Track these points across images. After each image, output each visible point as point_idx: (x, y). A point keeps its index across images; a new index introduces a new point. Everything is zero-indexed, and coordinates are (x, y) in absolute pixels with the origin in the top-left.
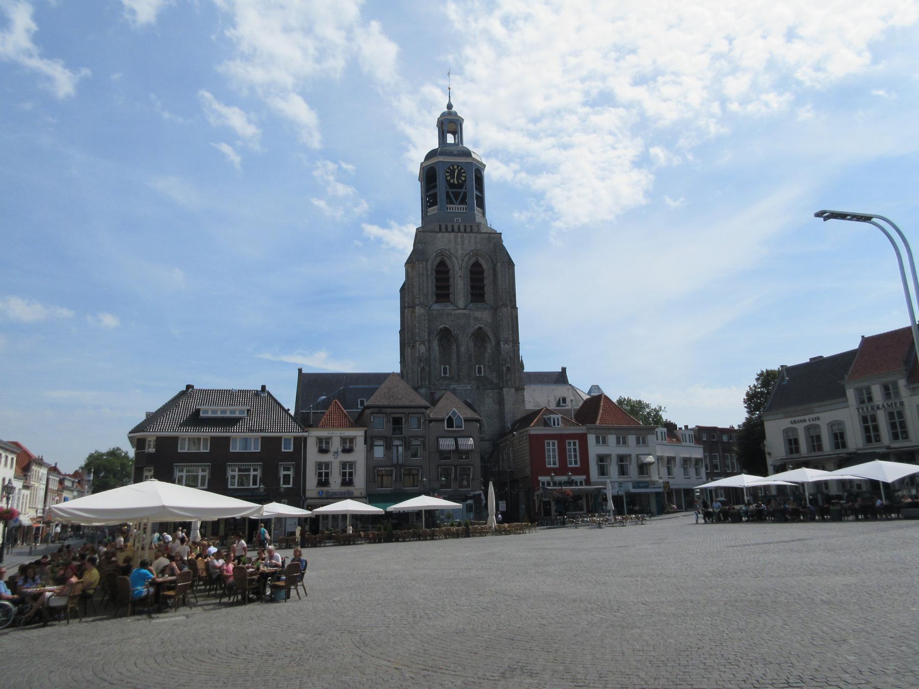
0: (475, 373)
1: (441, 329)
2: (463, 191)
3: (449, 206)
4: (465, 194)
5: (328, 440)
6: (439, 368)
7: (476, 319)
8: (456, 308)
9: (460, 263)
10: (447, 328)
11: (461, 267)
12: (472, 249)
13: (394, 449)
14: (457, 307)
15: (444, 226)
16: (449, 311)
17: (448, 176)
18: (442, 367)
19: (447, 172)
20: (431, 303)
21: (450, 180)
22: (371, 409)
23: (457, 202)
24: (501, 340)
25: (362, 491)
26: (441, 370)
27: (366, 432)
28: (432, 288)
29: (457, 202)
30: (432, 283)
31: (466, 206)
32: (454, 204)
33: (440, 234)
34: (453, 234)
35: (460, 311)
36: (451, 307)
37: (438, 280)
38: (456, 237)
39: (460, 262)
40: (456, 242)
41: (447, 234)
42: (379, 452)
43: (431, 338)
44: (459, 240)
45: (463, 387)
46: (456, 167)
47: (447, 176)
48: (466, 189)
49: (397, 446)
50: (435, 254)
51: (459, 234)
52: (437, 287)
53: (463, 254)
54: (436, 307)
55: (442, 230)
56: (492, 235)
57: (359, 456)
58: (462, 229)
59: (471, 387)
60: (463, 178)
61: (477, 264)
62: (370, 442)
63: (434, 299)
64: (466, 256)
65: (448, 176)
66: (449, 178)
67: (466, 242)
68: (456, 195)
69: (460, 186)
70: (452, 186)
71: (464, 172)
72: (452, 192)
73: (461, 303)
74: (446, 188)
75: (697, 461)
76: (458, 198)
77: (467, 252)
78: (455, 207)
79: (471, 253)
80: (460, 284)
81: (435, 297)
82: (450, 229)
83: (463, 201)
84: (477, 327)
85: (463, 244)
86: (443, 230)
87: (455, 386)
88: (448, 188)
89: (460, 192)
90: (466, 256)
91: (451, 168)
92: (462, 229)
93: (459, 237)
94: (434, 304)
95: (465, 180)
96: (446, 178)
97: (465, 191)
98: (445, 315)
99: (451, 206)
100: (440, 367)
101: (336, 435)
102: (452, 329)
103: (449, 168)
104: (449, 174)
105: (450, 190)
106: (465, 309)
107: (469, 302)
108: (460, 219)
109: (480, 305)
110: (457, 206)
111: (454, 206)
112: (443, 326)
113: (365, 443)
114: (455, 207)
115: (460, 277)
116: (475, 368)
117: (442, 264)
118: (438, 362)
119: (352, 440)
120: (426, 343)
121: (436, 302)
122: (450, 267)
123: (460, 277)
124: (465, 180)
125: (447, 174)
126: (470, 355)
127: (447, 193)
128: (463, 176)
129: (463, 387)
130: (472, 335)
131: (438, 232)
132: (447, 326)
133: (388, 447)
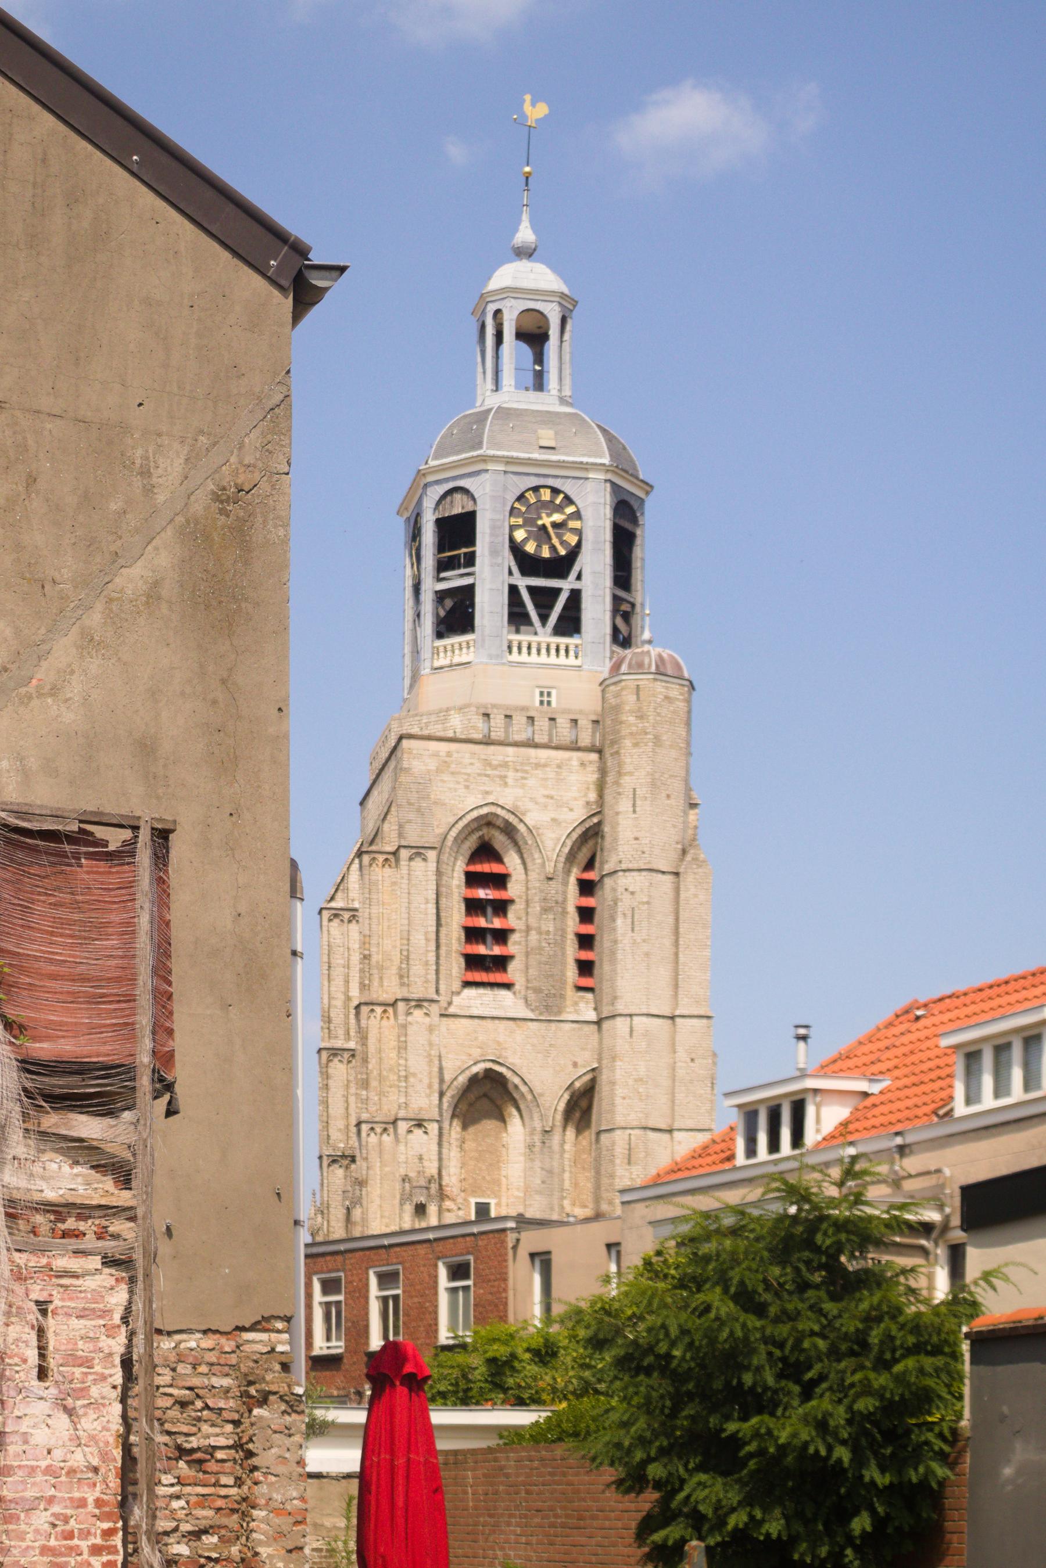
4: (575, 596)
17: (519, 527)
29: (544, 618)
46: (546, 495)
47: (513, 528)
48: (579, 577)
60: (573, 540)
66: (520, 535)
68: (544, 598)
69: (561, 566)
70: (527, 564)
74: (510, 573)
76: (551, 607)
78: (539, 644)
88: (515, 570)
89: (557, 592)
96: (512, 540)
97: (577, 585)
104: (520, 521)
105: (523, 583)
114: (539, 644)
124: (579, 545)
125: (513, 521)
127: (513, 590)
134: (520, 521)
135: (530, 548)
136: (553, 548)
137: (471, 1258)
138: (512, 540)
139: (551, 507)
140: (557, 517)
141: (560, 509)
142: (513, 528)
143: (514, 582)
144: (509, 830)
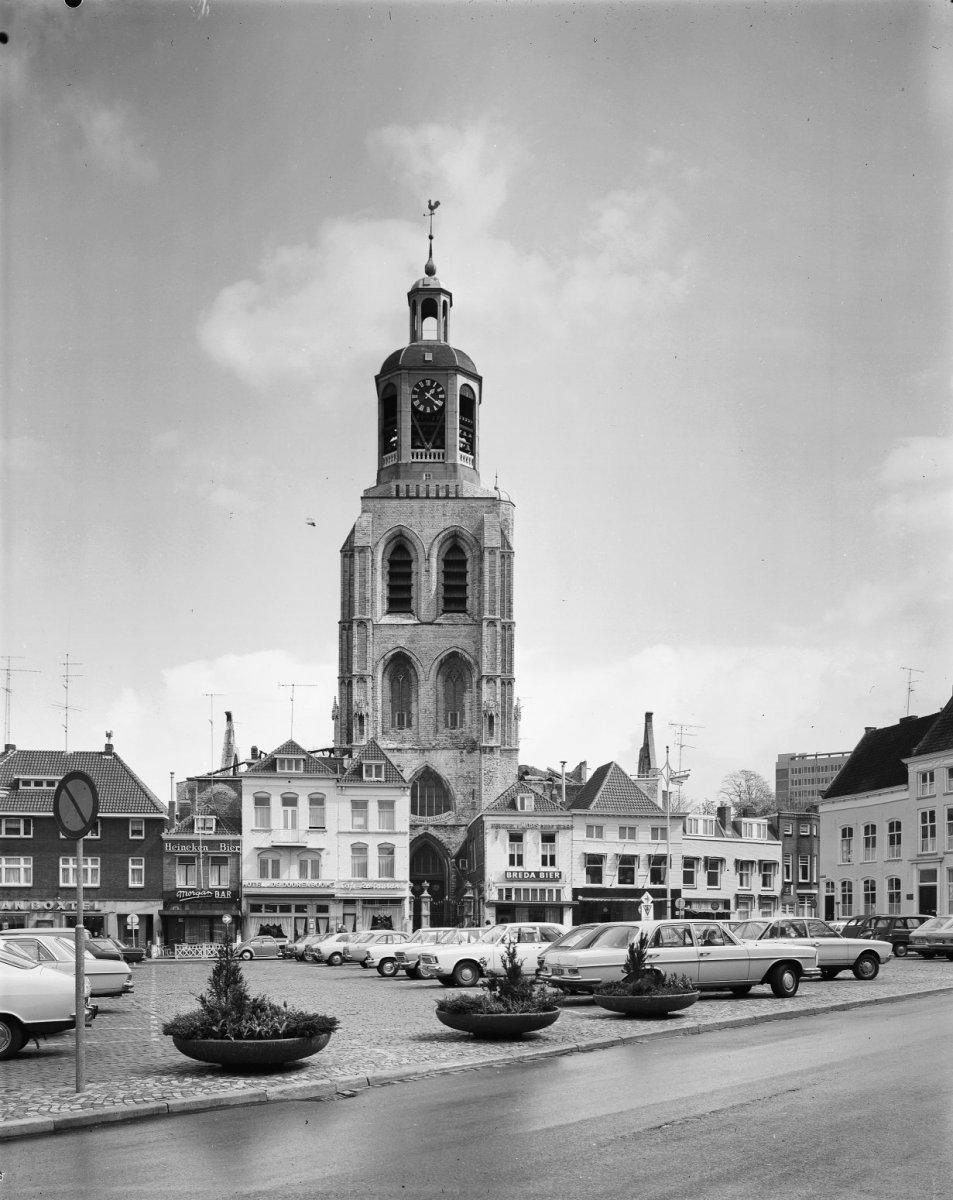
15: (405, 488)
17: (415, 399)
19: (414, 392)
21: (419, 406)
46: (428, 383)
55: (401, 495)
63: (386, 607)
65: (415, 399)
66: (416, 403)
75: (766, 867)
80: (428, 581)
95: (444, 405)
104: (416, 396)
109: (458, 617)
121: (389, 612)
122: (413, 555)
124: (444, 405)
128: (441, 399)
135: (421, 408)
138: (413, 405)
139: (427, 389)
140: (432, 391)
141: (431, 387)
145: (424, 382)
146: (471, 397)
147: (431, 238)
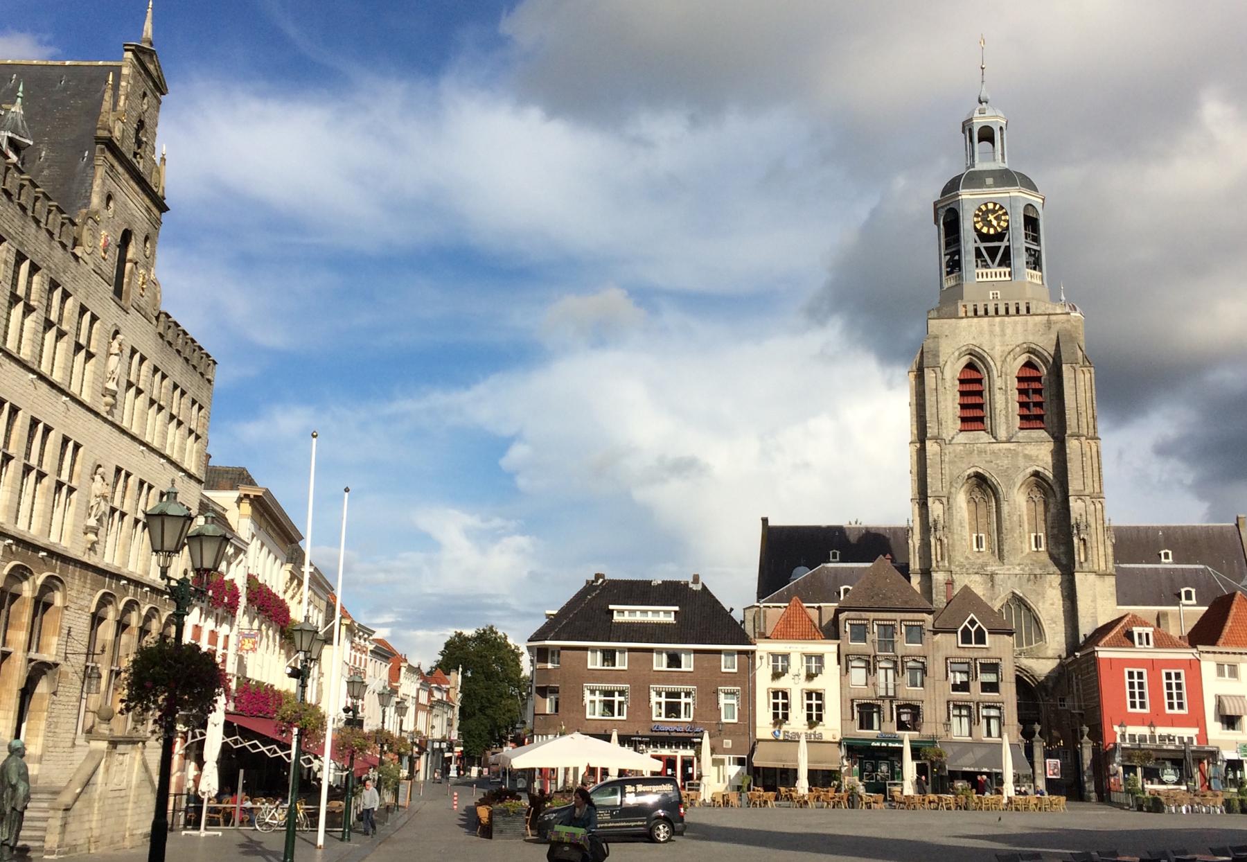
0: (1030, 545)
1: (968, 475)
2: (1004, 244)
3: (980, 271)
4: (1007, 249)
5: (786, 657)
6: (968, 537)
7: (1028, 457)
8: (994, 441)
9: (999, 368)
10: (980, 473)
11: (1001, 372)
12: (1020, 342)
13: (881, 673)
14: (995, 438)
15: (972, 308)
16: (983, 446)
17: (978, 222)
18: (974, 536)
19: (977, 216)
20: (952, 433)
22: (846, 613)
23: (993, 262)
24: (1070, 494)
25: (834, 732)
26: (972, 541)
27: (839, 646)
28: (954, 408)
29: (993, 262)
30: (954, 400)
31: (1009, 269)
32: (986, 266)
33: (965, 320)
34: (986, 319)
35: (1001, 445)
36: (984, 437)
37: (963, 394)
38: (992, 325)
39: (999, 364)
40: (992, 333)
41: (976, 320)
42: (858, 675)
43: (953, 490)
44: (997, 329)
45: (1009, 569)
48: (1009, 240)
49: (886, 669)
50: (957, 354)
51: (998, 319)
52: (963, 407)
53: (1003, 352)
54: (962, 438)
55: (969, 314)
56: (1053, 318)
57: (829, 682)
58: (1002, 311)
59: (1021, 570)
60: (1004, 224)
61: (1029, 365)
62: (844, 660)
64: (1009, 353)
66: (978, 226)
67: (1009, 331)
68: (993, 252)
69: (999, 236)
70: (984, 237)
71: (1006, 214)
72: (985, 248)
73: (1002, 433)
74: (976, 242)
77: (1010, 348)
78: (991, 273)
79: (1018, 349)
81: (959, 422)
82: (981, 312)
83: (1006, 260)
84: (1030, 470)
85: (1003, 334)
86: (971, 313)
87: (994, 568)
90: (1009, 353)
91: (984, 208)
92: (1002, 311)
93: (997, 325)
94: (957, 434)
95: (1008, 226)
96: (976, 229)
97: (1008, 244)
98: (976, 452)
99: (984, 271)
100: (971, 536)
101: (797, 650)
102: (987, 475)
103: (980, 210)
105: (982, 246)
106: (1008, 441)
107: (1017, 429)
108: (998, 292)
110: (993, 270)
111: (989, 271)
112: (973, 470)
113: (839, 663)
114: (991, 273)
115: (1000, 389)
116: (1030, 538)
117: (970, 366)
118: (967, 527)
119: (820, 658)
120: (945, 500)
123: (1000, 389)
124: (1008, 226)
126: (1020, 516)
127: (978, 250)
128: (1004, 221)
129: (1009, 569)
130: (1022, 485)
131: (962, 318)
132: (980, 471)
133: (871, 668)
134: (979, 219)
135: (985, 230)
136: (995, 228)
137: (972, 615)
138: (976, 229)
142: (975, 223)
143: (976, 245)
144: (982, 359)
145: (986, 205)
146: (1035, 216)
147: (983, 82)
